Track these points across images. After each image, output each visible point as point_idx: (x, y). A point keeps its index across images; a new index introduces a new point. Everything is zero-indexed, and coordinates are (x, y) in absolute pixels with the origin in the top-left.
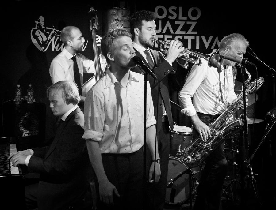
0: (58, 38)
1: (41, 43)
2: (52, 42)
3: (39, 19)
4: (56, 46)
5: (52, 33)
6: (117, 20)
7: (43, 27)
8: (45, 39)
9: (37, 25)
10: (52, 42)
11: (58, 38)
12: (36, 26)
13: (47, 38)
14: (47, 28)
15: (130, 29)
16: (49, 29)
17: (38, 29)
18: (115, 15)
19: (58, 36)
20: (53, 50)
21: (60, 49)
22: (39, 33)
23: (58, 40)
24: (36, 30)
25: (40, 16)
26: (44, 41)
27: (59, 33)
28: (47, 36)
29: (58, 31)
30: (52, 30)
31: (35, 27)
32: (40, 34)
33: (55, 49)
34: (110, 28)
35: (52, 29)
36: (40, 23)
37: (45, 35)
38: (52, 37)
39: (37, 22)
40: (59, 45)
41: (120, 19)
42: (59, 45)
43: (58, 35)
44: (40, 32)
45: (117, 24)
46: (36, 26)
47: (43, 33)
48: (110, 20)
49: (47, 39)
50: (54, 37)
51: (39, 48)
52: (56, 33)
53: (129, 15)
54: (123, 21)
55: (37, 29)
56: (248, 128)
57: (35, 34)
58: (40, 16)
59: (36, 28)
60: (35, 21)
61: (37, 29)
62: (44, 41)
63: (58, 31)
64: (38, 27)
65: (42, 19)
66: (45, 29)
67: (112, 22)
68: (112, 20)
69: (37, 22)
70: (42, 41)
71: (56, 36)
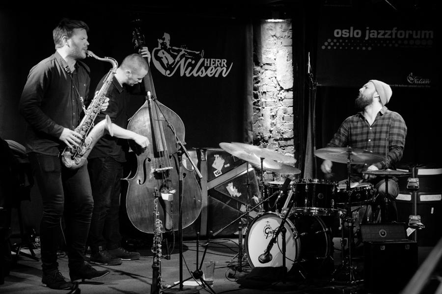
0: (190, 60)
1: (166, 65)
2: (180, 65)
4: (186, 70)
5: (181, 53)
6: (274, 37)
7: (169, 47)
8: (171, 61)
9: (161, 44)
10: (180, 65)
11: (190, 60)
12: (160, 46)
13: (173, 61)
14: (173, 48)
15: (291, 47)
16: (177, 49)
18: (271, 30)
19: (189, 58)
20: (182, 74)
21: (193, 74)
22: (164, 54)
23: (189, 62)
24: (159, 50)
25: (165, 34)
26: (170, 63)
27: (189, 54)
28: (174, 57)
29: (189, 51)
30: (181, 51)
31: (157, 47)
32: (164, 55)
33: (185, 74)
34: (265, 46)
35: (181, 49)
36: (164, 41)
37: (171, 56)
38: (181, 58)
39: (160, 41)
40: (190, 68)
41: (278, 35)
42: (190, 68)
43: (189, 56)
44: (165, 52)
45: (275, 41)
46: (160, 46)
47: (169, 53)
48: (265, 37)
49: (175, 61)
50: (184, 59)
51: (163, 71)
52: (186, 53)
53: (290, 29)
54: (282, 37)
55: (160, 48)
57: (158, 55)
58: (165, 34)
59: (159, 48)
60: (158, 40)
61: (160, 48)
62: (170, 63)
63: (189, 51)
64: (161, 47)
65: (167, 37)
66: (172, 49)
67: (267, 40)
68: (266, 37)
69: (160, 41)
70: (168, 64)
71: (186, 58)
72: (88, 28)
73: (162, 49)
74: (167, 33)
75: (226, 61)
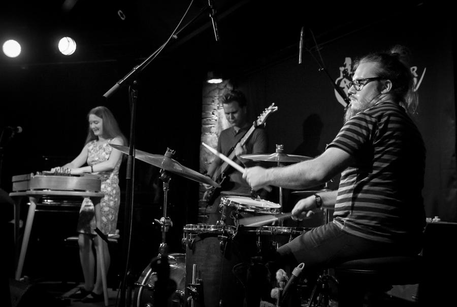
3: (344, 64)
12: (342, 74)
17: (343, 78)
22: (345, 82)
31: (339, 76)
36: (346, 68)
39: (342, 69)
46: (342, 74)
56: (52, 211)
69: (342, 69)
72: (388, 80)
73: (344, 77)
74: (348, 57)
75: (416, 68)
